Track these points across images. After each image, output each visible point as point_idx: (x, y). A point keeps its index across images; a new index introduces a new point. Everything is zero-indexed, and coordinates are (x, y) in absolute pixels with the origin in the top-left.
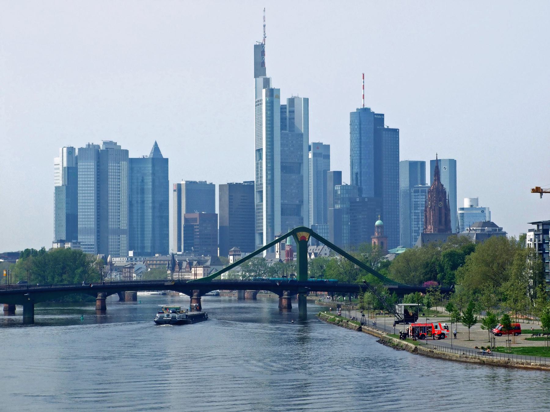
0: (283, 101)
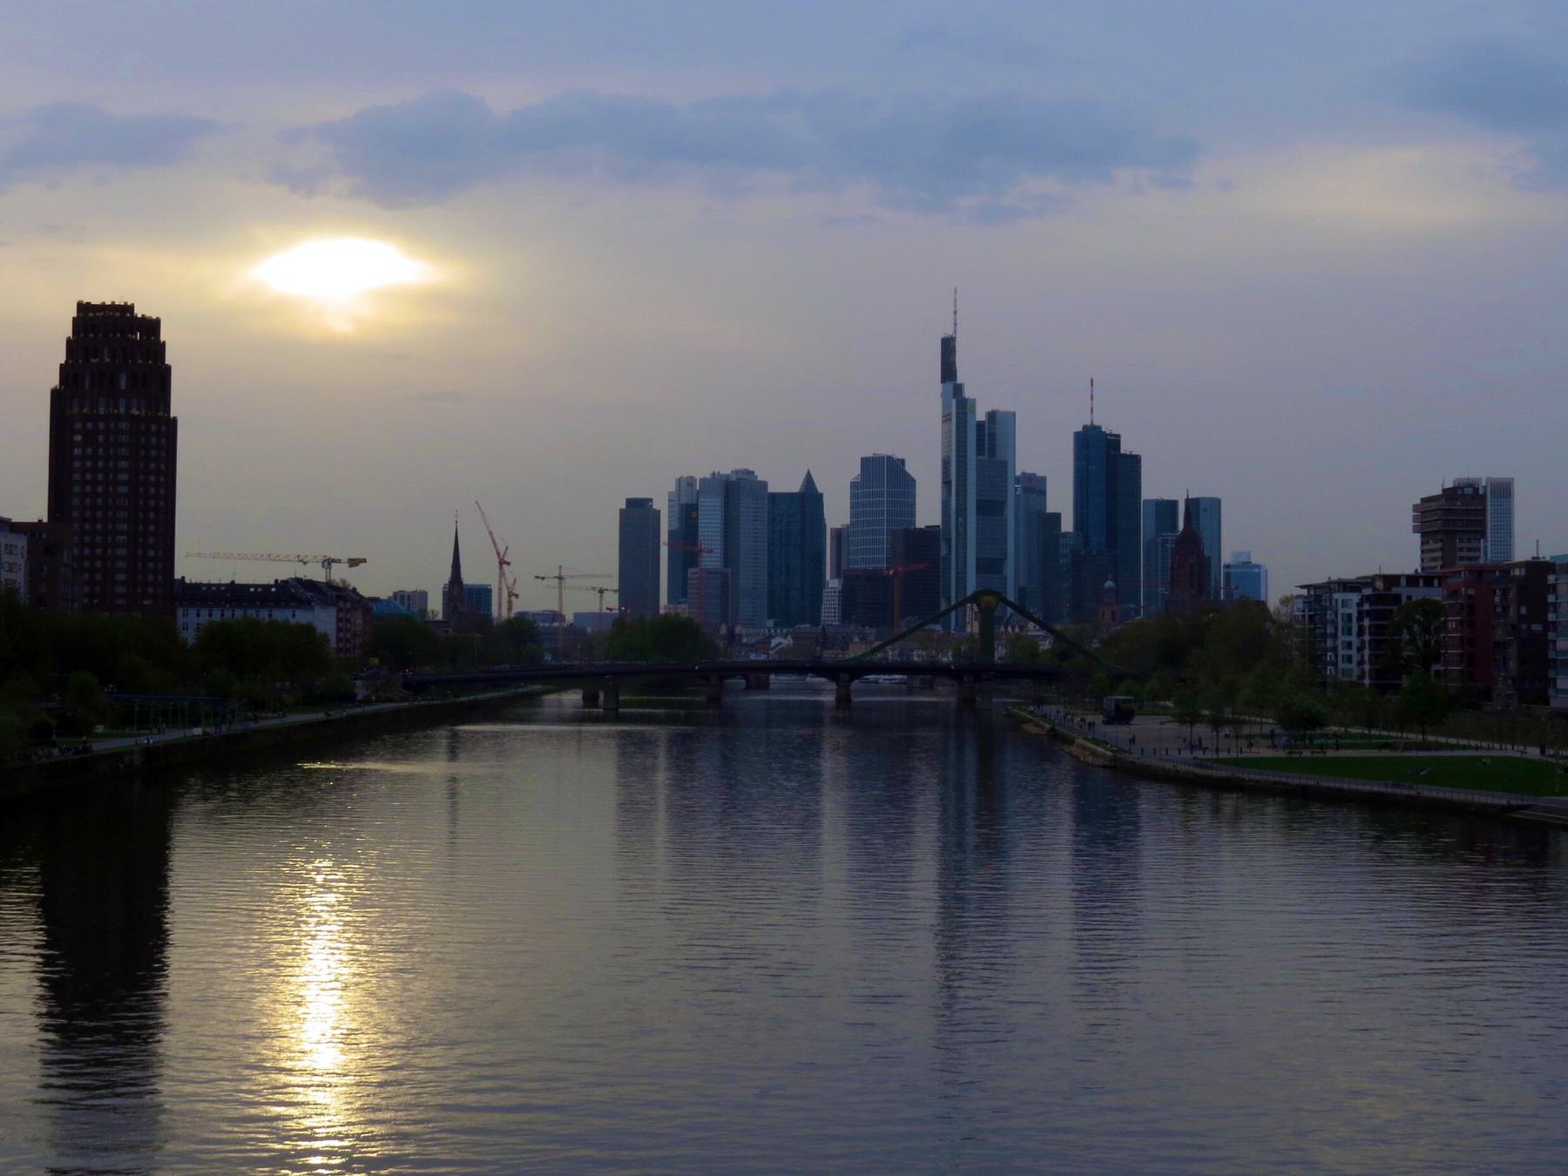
0: (981, 416)
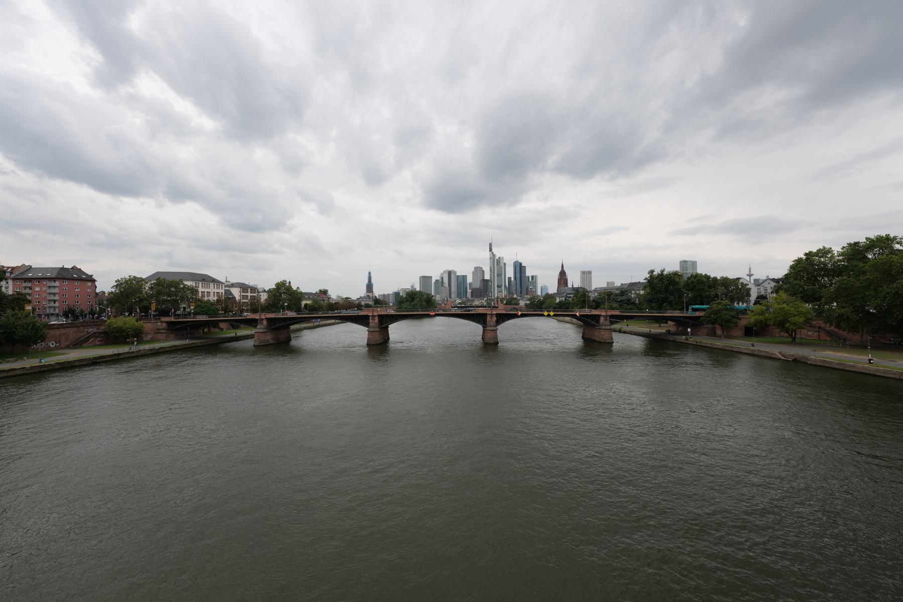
0: (497, 258)
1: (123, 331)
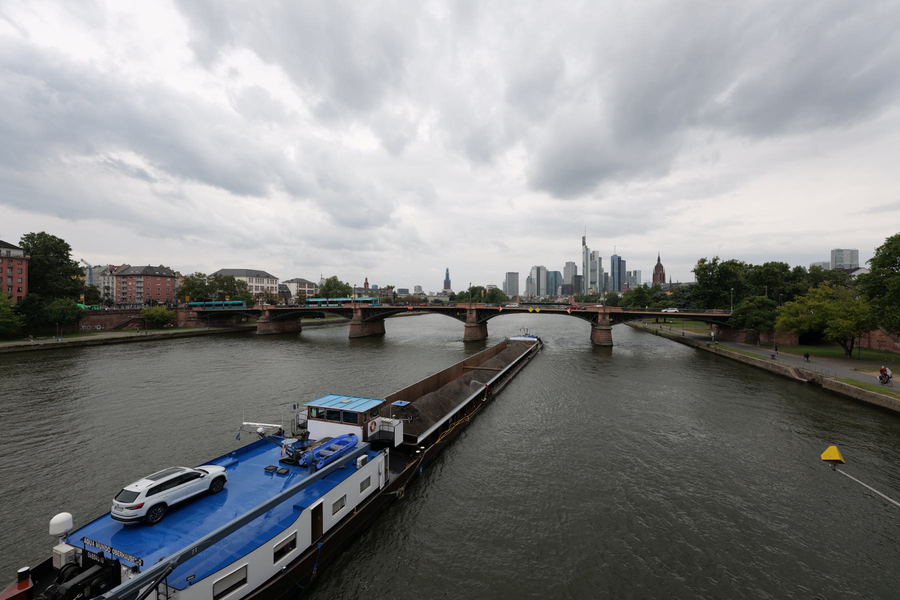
0: (591, 252)
1: (154, 318)
